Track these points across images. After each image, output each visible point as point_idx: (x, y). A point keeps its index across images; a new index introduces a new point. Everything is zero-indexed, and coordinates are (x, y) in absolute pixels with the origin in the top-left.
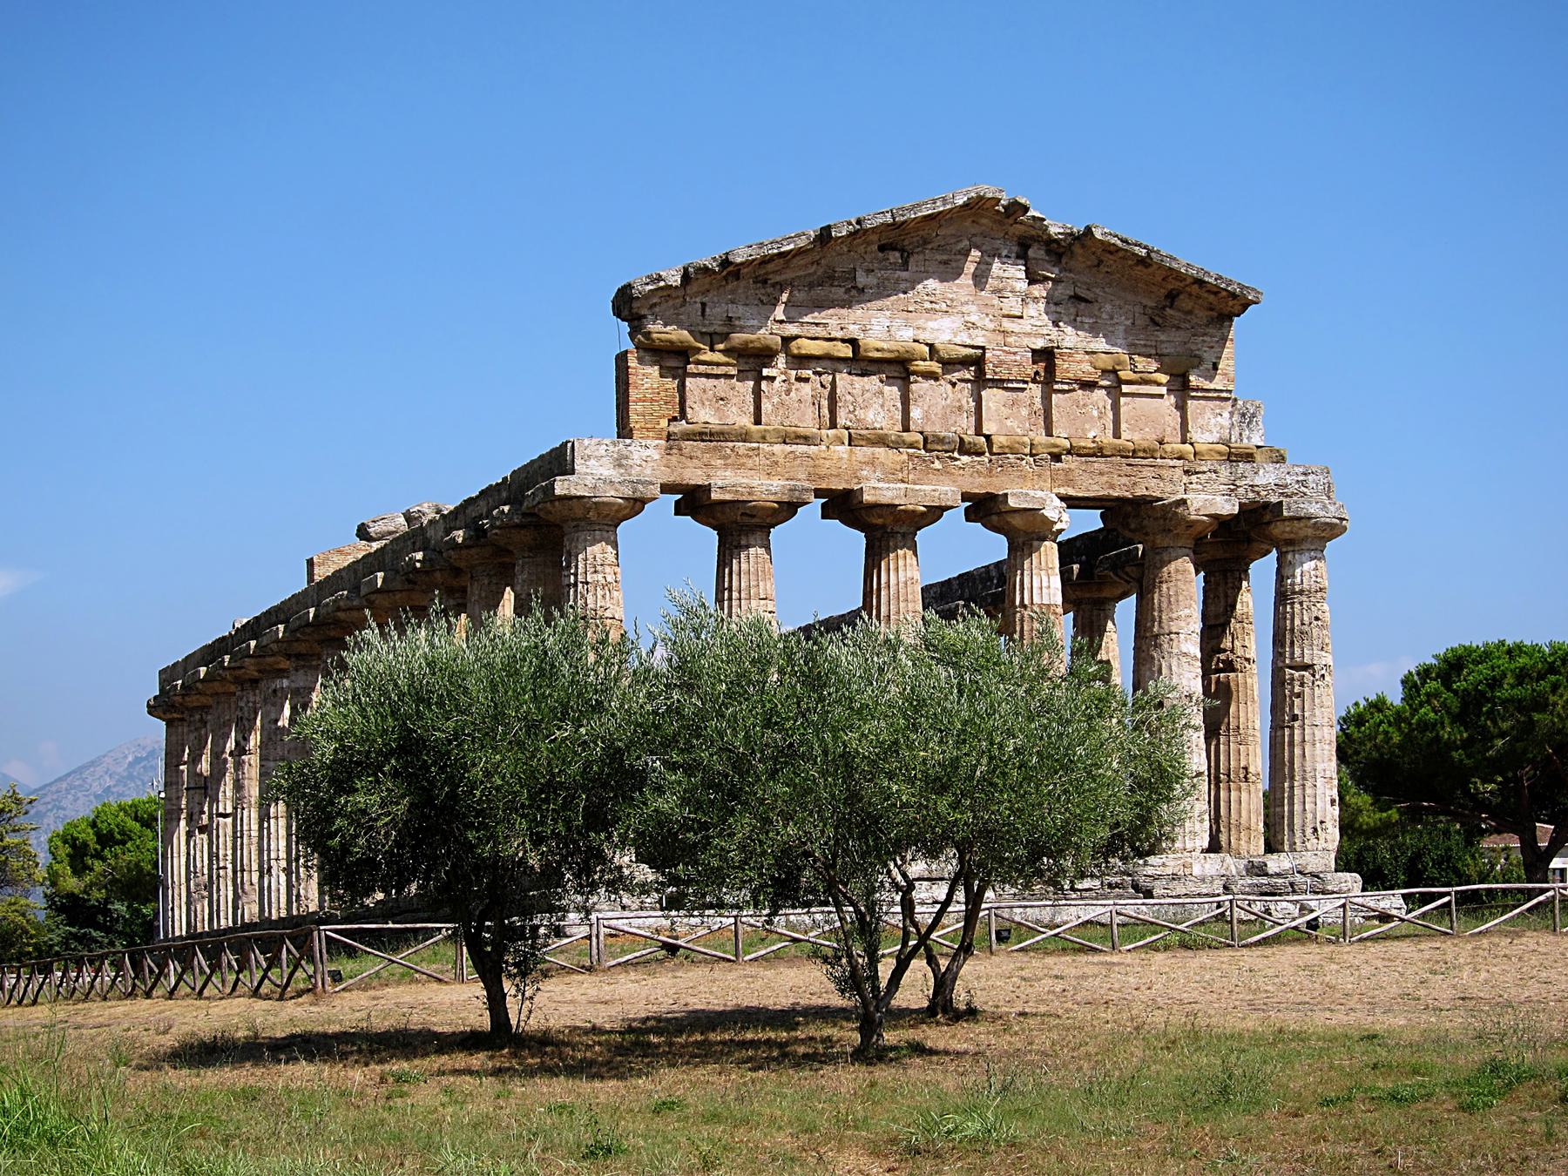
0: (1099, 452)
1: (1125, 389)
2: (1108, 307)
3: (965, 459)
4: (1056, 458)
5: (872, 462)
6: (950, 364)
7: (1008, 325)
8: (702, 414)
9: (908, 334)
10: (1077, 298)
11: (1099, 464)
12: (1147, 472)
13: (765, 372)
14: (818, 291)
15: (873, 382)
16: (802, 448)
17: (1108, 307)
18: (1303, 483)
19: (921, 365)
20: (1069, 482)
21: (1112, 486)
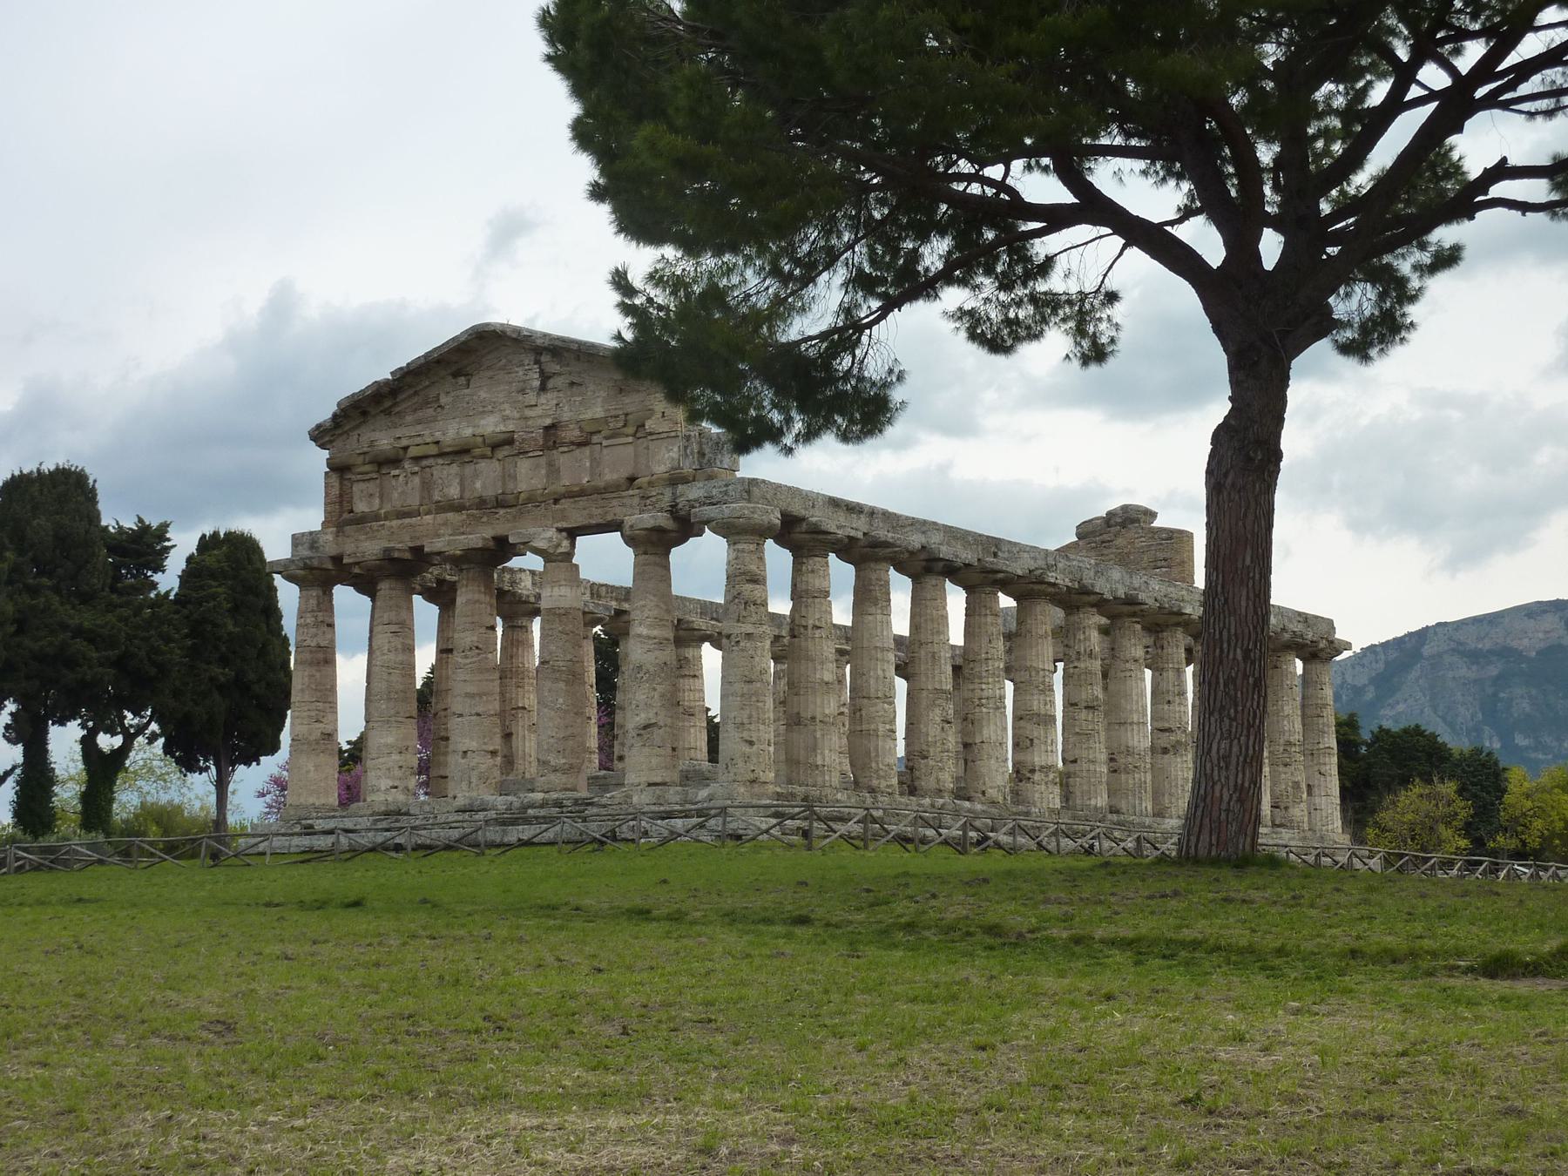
0: (582, 493)
1: (605, 443)
2: (592, 387)
3: (502, 511)
4: (556, 501)
5: (445, 524)
6: (495, 446)
7: (528, 413)
8: (361, 507)
9: (468, 432)
10: (572, 384)
11: (583, 502)
12: (615, 502)
13: (394, 472)
14: (420, 414)
15: (454, 469)
16: (407, 521)
17: (592, 387)
18: (726, 493)
19: (477, 451)
20: (564, 518)
21: (591, 516)
